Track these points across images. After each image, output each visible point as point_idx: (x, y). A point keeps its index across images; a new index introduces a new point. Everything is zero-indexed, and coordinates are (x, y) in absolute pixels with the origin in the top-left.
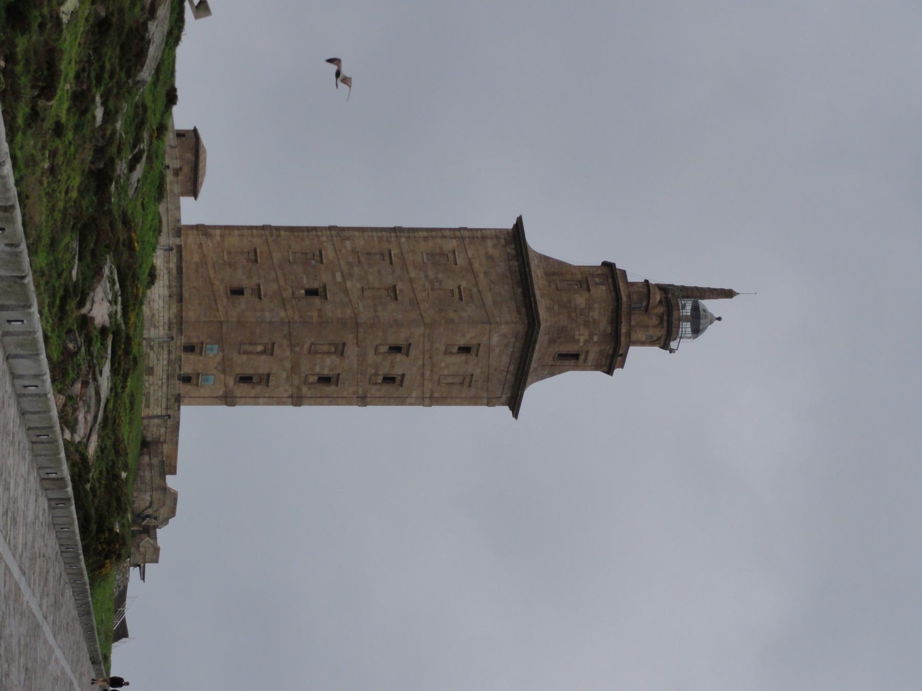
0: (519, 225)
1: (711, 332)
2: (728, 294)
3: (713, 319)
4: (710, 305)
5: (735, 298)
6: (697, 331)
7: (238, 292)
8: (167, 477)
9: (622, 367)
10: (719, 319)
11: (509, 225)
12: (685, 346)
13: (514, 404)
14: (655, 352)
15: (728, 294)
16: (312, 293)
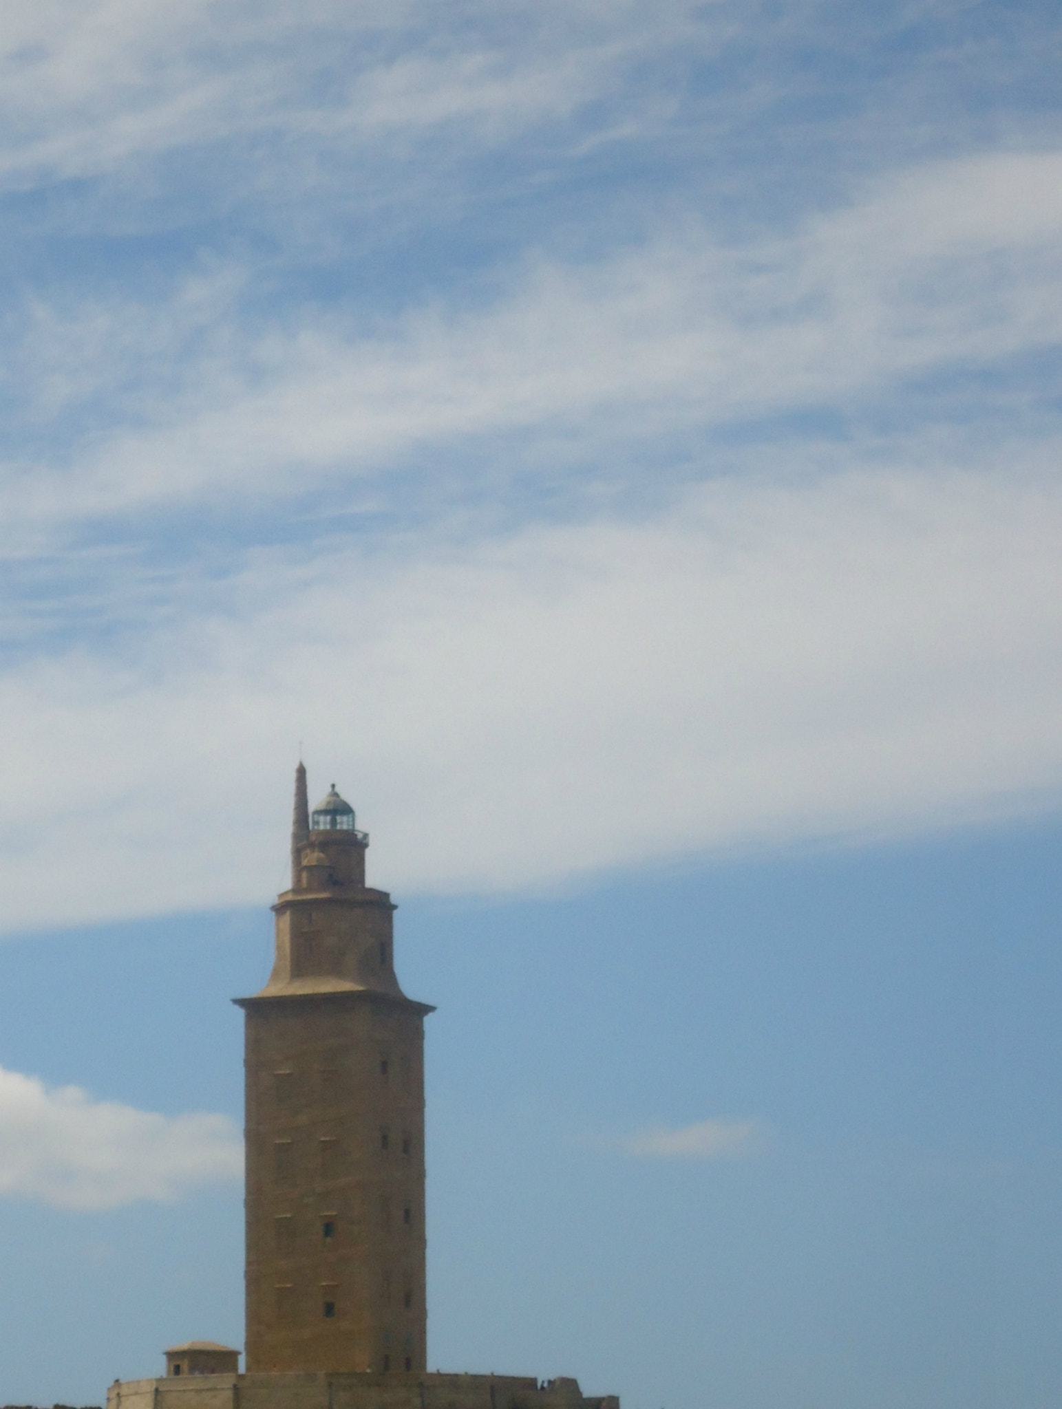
0: (241, 1002)
1: (347, 796)
2: (301, 772)
3: (335, 794)
4: (317, 798)
5: (306, 765)
6: (346, 810)
7: (329, 1309)
8: (431, 1367)
9: (386, 895)
10: (333, 786)
11: (240, 1014)
12: (362, 824)
13: (424, 1009)
14: (372, 858)
15: (301, 772)
16: (329, 1229)
